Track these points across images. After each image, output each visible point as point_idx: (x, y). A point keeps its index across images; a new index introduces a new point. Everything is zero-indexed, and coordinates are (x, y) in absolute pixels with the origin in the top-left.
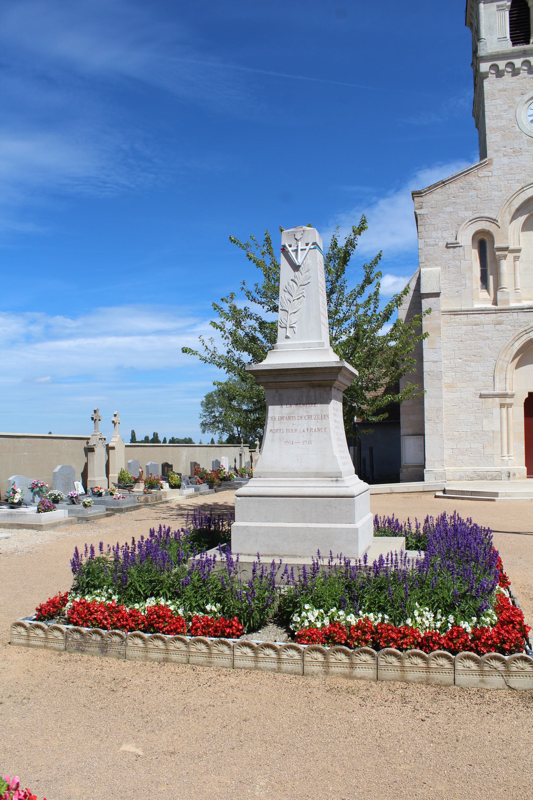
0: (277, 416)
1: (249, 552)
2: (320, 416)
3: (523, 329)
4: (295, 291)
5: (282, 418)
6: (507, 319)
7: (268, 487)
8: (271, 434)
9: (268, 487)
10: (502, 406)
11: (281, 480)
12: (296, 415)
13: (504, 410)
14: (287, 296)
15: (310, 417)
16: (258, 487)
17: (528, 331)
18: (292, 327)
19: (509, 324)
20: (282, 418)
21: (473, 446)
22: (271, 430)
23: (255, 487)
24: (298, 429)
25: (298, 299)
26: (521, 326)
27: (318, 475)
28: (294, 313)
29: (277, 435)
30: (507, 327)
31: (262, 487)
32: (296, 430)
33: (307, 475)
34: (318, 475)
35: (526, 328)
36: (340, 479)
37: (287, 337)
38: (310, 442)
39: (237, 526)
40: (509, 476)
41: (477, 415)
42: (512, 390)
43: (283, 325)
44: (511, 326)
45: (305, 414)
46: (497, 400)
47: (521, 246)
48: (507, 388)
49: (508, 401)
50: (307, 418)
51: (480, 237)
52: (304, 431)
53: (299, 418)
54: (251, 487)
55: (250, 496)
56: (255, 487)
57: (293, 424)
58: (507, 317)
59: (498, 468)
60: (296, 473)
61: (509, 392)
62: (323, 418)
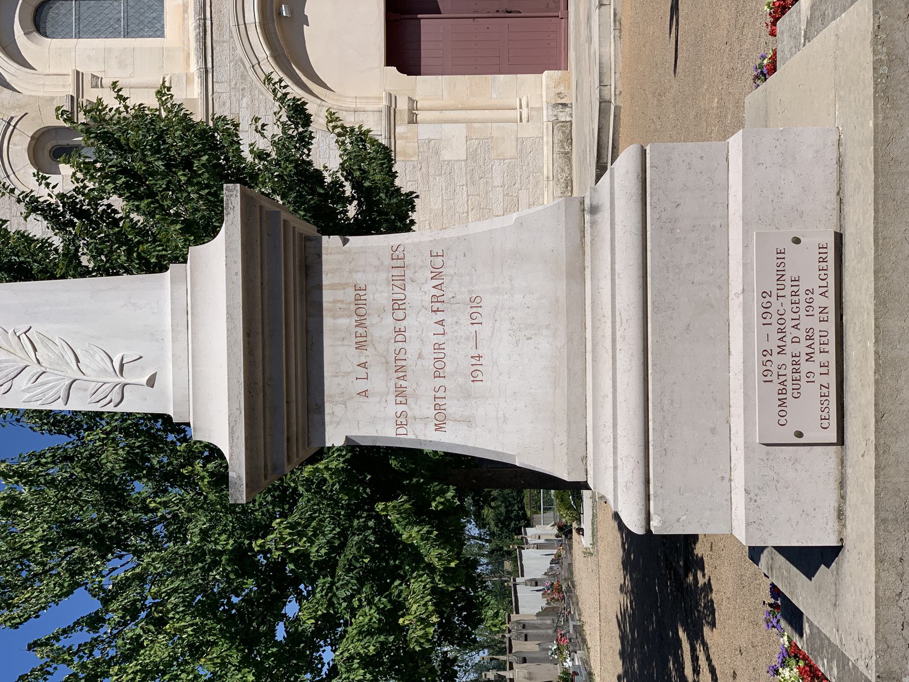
0: (393, 409)
1: (833, 485)
2: (396, 272)
3: (251, 72)
4: (12, 357)
5: (400, 392)
6: (228, 105)
7: (615, 425)
8: (449, 426)
9: (615, 425)
10: (413, 120)
11: (594, 386)
12: (393, 347)
13: (421, 116)
14: (22, 382)
15: (398, 305)
16: (615, 461)
17: (255, 62)
18: (122, 366)
19: (239, 101)
20: (400, 392)
21: (498, 181)
22: (438, 428)
23: (615, 468)
24: (436, 339)
25: (35, 350)
26: (243, 77)
27: (576, 270)
28: (78, 361)
29: (453, 407)
30: (244, 105)
31: (615, 448)
32: (438, 347)
33: (575, 308)
34: (576, 270)
35: (248, 65)
36: (587, 202)
37: (151, 382)
38: (475, 302)
39: (748, 524)
40: (564, 105)
41: (432, 171)
42: (380, 98)
43: (115, 396)
44: (243, 96)
45: (389, 320)
46: (399, 129)
47: (70, 71)
48: (376, 107)
49: (403, 105)
50: (400, 314)
51: (45, 156)
52: (441, 323)
53: (399, 338)
54: (615, 482)
55: (647, 482)
56: (615, 468)
57: (420, 356)
58: (224, 103)
59: (547, 127)
60: (570, 339)
61: (385, 103)
62: (399, 263)
